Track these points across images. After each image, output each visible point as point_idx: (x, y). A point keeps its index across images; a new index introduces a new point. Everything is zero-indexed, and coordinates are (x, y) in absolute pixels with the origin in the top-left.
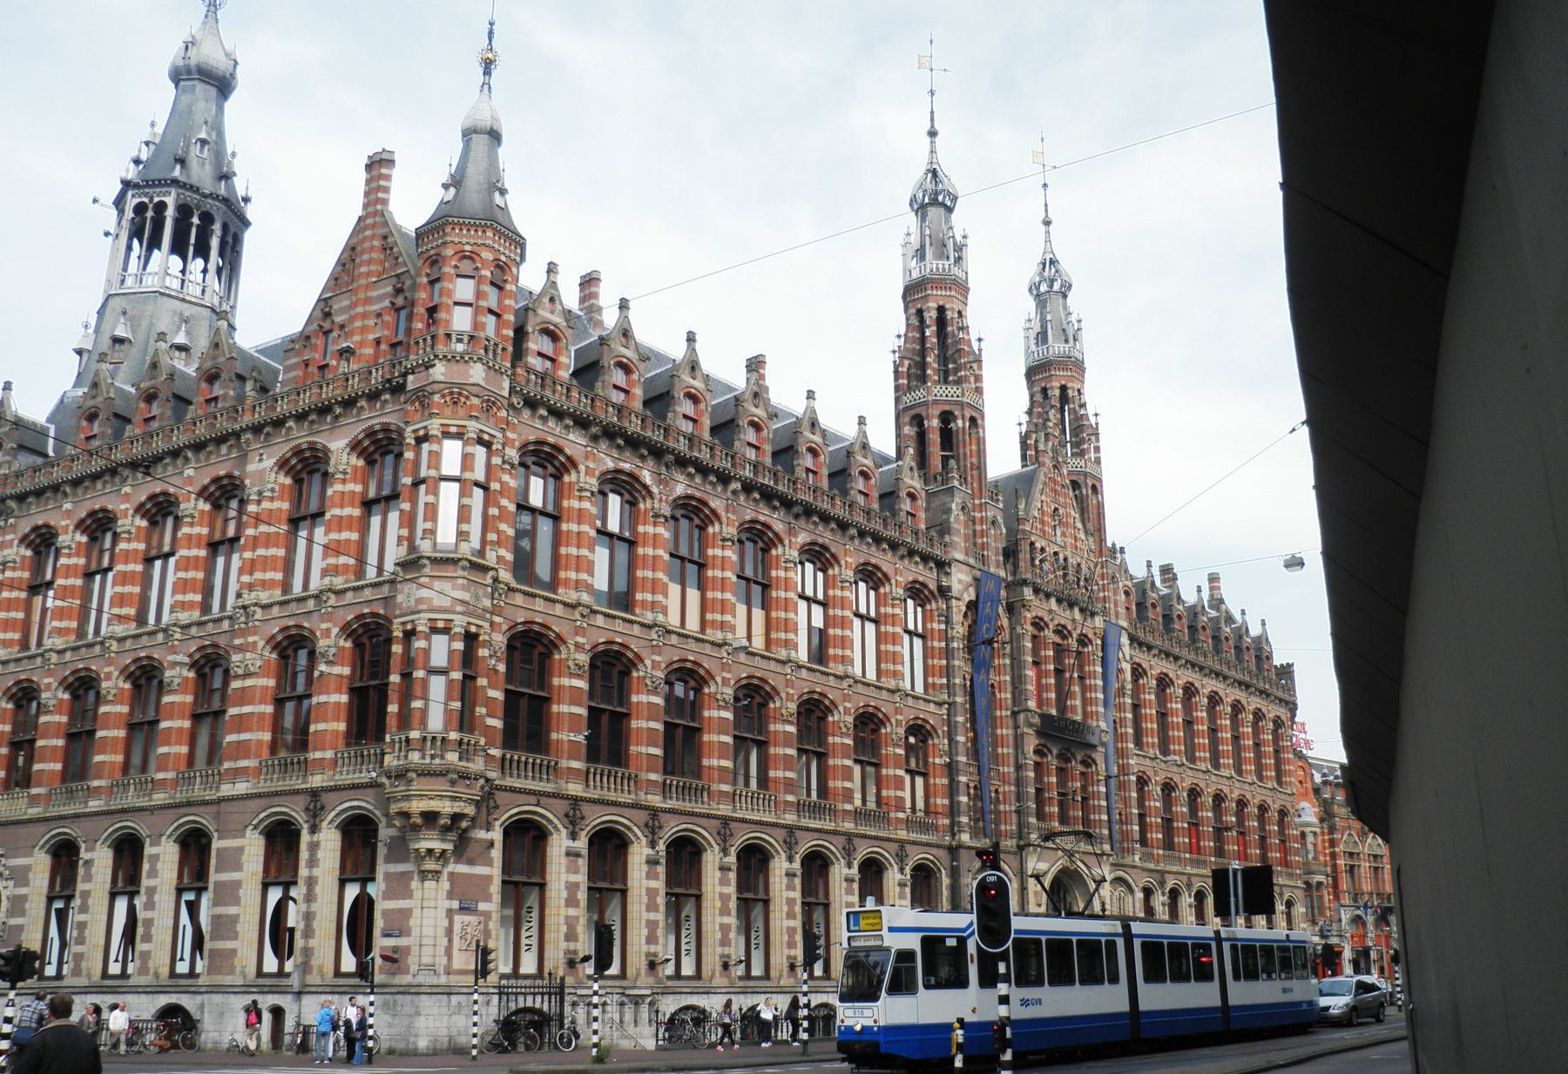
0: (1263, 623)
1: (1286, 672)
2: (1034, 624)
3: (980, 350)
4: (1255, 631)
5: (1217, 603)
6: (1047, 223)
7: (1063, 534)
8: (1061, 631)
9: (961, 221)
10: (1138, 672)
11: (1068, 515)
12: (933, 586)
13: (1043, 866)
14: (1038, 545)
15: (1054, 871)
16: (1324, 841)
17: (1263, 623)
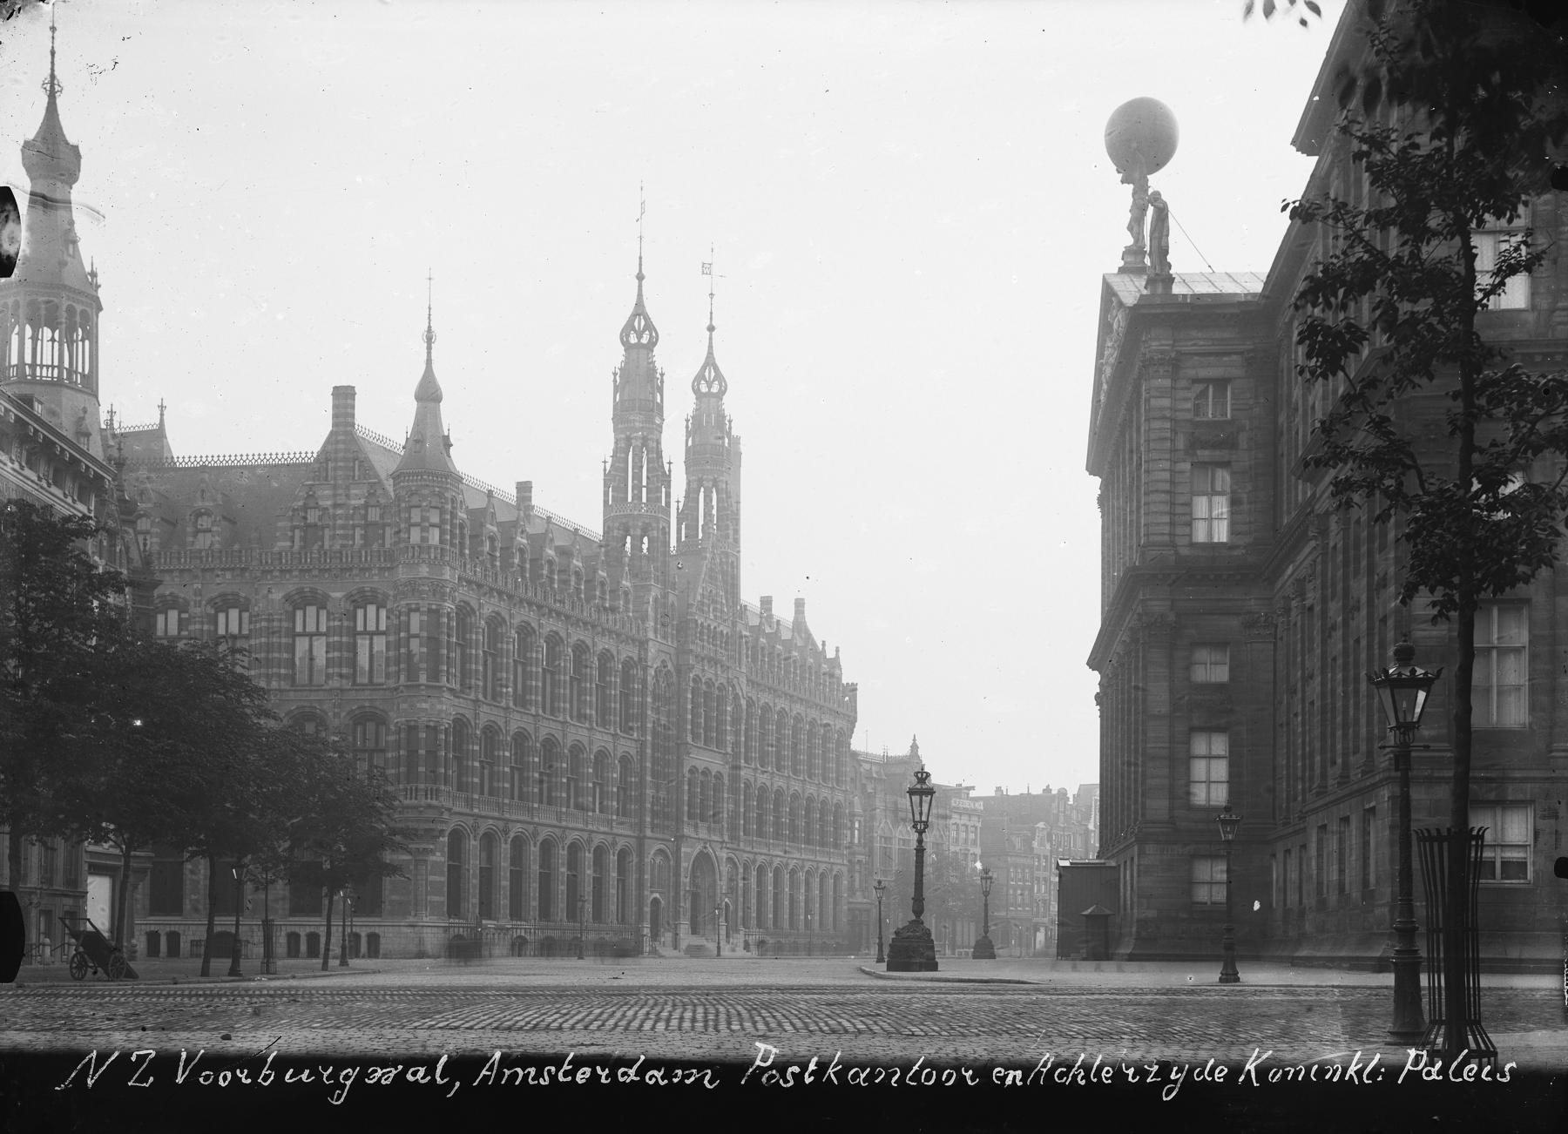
0: (837, 650)
1: (853, 689)
2: (694, 680)
3: (670, 471)
4: (830, 654)
5: (799, 625)
6: (711, 329)
7: (715, 610)
8: (709, 684)
9: (660, 356)
10: (750, 703)
11: (717, 594)
12: (636, 659)
13: (689, 850)
14: (699, 622)
15: (695, 854)
16: (865, 826)
17: (837, 650)
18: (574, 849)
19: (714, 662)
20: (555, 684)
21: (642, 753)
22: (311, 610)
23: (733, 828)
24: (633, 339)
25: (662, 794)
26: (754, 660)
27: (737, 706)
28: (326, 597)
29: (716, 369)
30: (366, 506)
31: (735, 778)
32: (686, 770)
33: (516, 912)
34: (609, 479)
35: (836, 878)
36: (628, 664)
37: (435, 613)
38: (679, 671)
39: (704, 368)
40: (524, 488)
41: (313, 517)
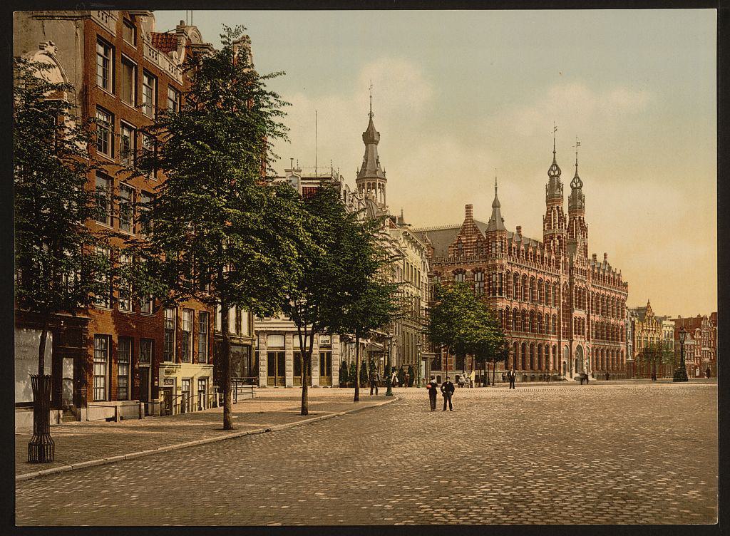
5: (606, 263)
18: (540, 346)
19: (582, 281)
20: (533, 293)
21: (559, 313)
22: (460, 275)
23: (588, 336)
24: (552, 174)
25: (566, 326)
26: (593, 278)
27: (588, 294)
28: (465, 271)
29: (557, 166)
30: (477, 242)
31: (588, 319)
32: (574, 317)
33: (524, 368)
34: (545, 221)
35: (622, 352)
36: (555, 284)
37: (501, 274)
38: (570, 284)
39: (552, 166)
40: (519, 228)
41: (460, 246)
